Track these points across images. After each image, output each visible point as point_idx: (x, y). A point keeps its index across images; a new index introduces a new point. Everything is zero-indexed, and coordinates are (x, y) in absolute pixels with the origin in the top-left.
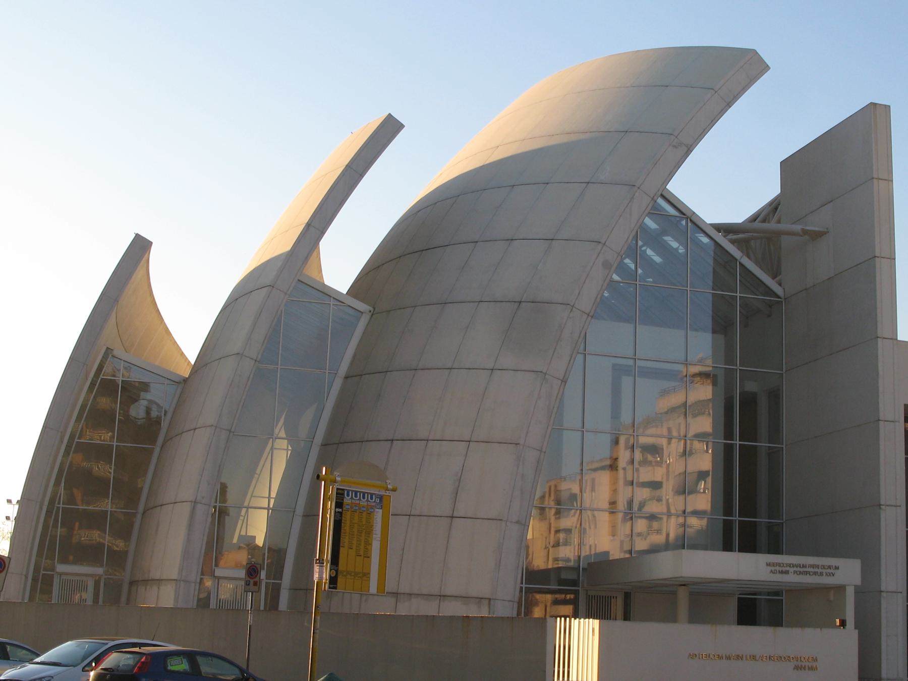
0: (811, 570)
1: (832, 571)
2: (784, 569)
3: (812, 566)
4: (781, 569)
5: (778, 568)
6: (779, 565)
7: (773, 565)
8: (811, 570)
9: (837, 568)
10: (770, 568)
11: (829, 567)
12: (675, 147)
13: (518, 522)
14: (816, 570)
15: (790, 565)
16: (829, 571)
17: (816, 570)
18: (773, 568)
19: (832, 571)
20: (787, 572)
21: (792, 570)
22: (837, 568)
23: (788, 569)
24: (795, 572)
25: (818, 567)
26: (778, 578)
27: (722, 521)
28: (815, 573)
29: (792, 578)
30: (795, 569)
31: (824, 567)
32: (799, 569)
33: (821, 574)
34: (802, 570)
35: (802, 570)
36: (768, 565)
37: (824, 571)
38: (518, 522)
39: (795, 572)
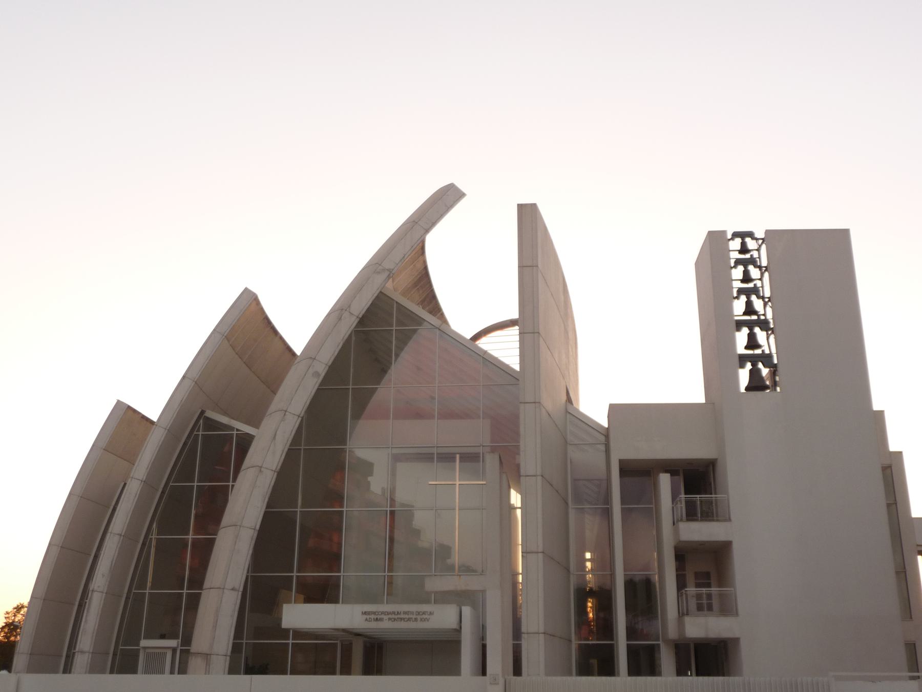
0: (407, 616)
2: (379, 617)
3: (405, 613)
4: (375, 617)
5: (373, 616)
6: (374, 613)
8: (407, 616)
9: (431, 613)
10: (365, 617)
11: (424, 613)
12: (379, 273)
13: (233, 589)
15: (383, 613)
16: (424, 616)
18: (368, 617)
20: (381, 620)
21: (386, 617)
22: (431, 613)
24: (390, 619)
25: (412, 613)
26: (373, 625)
28: (409, 619)
29: (386, 625)
30: (390, 616)
31: (419, 613)
32: (393, 616)
33: (416, 620)
35: (396, 617)
36: (365, 613)
37: (419, 617)
38: (233, 589)
39: (390, 619)
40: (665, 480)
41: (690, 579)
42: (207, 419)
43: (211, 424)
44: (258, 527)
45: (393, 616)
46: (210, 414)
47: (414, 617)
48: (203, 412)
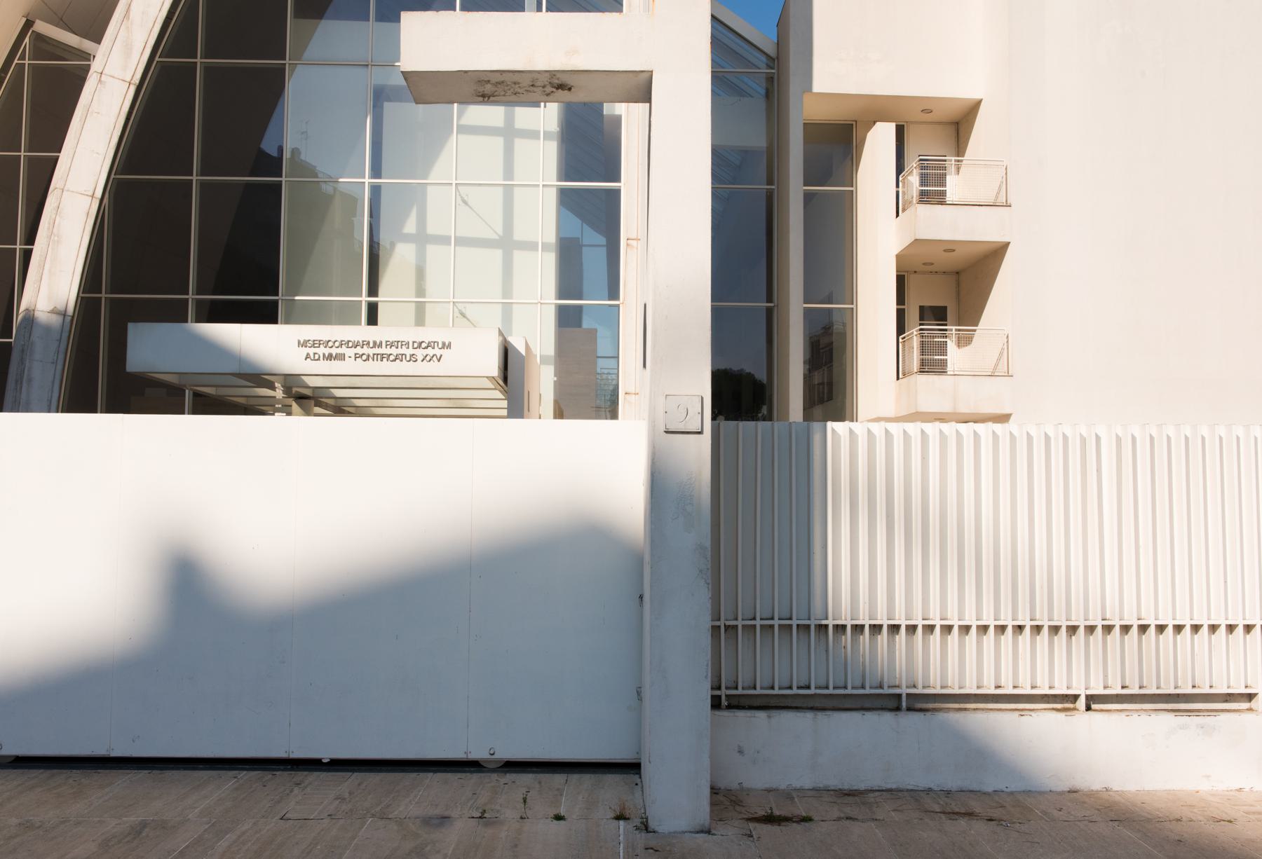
0: (394, 351)
1: (437, 352)
2: (334, 351)
4: (327, 351)
5: (322, 350)
7: (316, 344)
8: (394, 351)
10: (305, 351)
14: (403, 350)
16: (430, 351)
17: (403, 350)
18: (312, 351)
19: (437, 352)
20: (341, 357)
21: (350, 352)
23: (343, 350)
24: (357, 356)
27: (427, 293)
30: (359, 350)
32: (366, 350)
34: (371, 352)
37: (420, 353)
39: (357, 356)
40: (879, 142)
41: (913, 315)
42: (39, 37)
43: (44, 46)
44: (99, 194)
45: (366, 350)
46: (41, 27)
47: (409, 352)
48: (29, 24)
